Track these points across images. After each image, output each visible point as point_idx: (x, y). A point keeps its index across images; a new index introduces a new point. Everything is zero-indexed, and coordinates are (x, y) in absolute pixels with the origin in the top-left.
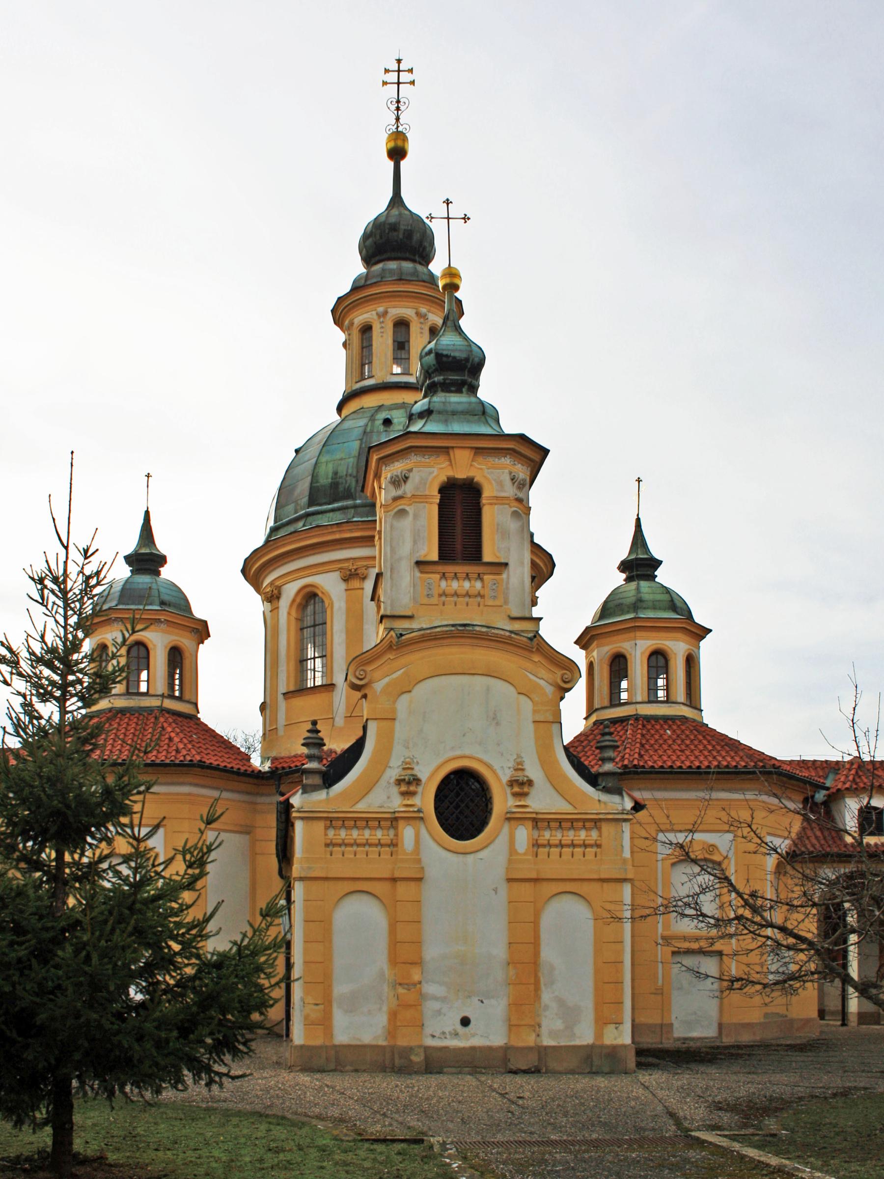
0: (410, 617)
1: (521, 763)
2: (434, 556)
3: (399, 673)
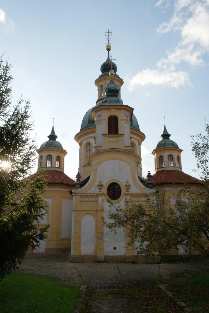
0: (101, 147)
1: (128, 181)
2: (107, 133)
3: (98, 160)
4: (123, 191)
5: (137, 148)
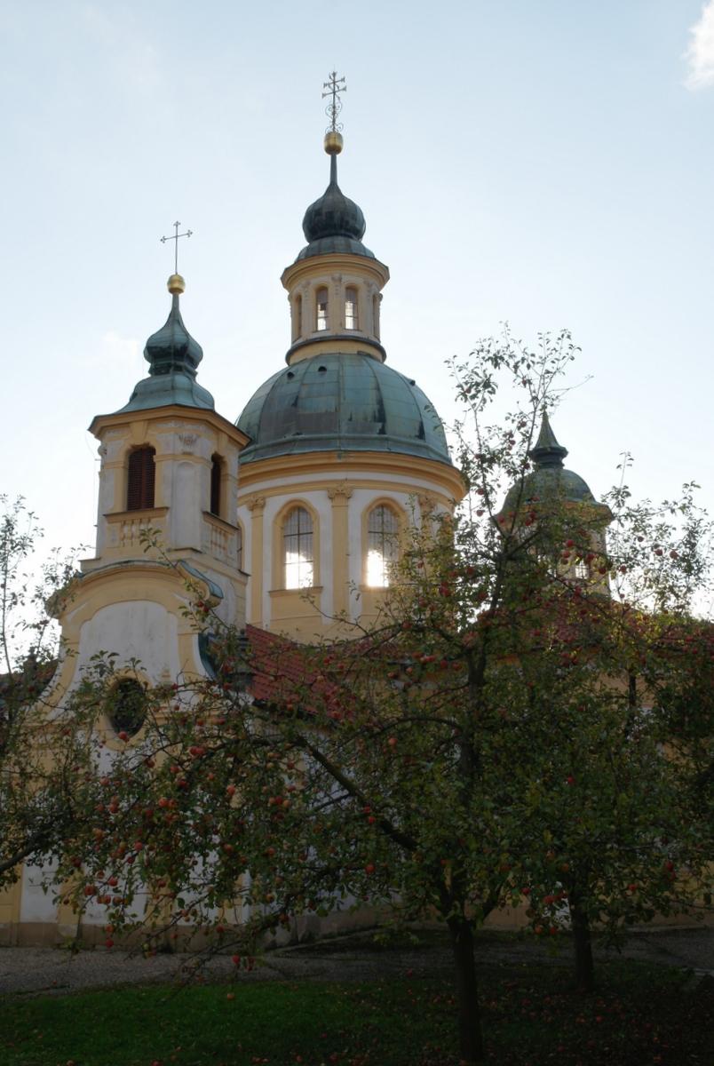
1: (167, 671)
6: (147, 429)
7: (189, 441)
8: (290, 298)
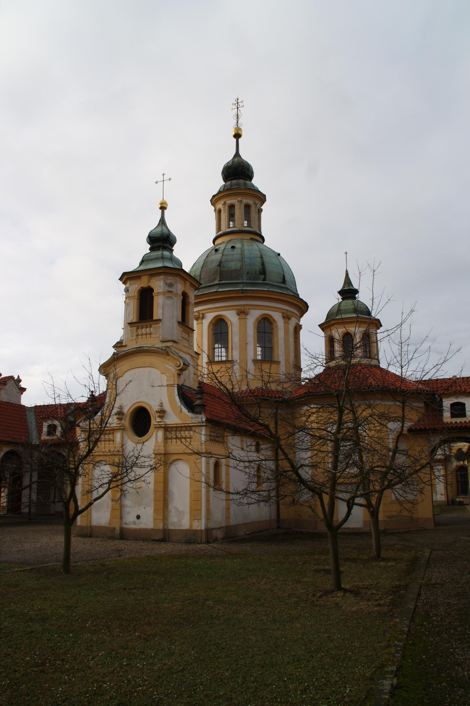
4: (155, 421)
5: (277, 326)
6: (150, 279)
7: (171, 285)
8: (215, 210)
